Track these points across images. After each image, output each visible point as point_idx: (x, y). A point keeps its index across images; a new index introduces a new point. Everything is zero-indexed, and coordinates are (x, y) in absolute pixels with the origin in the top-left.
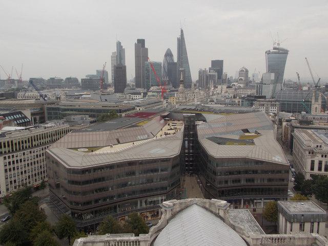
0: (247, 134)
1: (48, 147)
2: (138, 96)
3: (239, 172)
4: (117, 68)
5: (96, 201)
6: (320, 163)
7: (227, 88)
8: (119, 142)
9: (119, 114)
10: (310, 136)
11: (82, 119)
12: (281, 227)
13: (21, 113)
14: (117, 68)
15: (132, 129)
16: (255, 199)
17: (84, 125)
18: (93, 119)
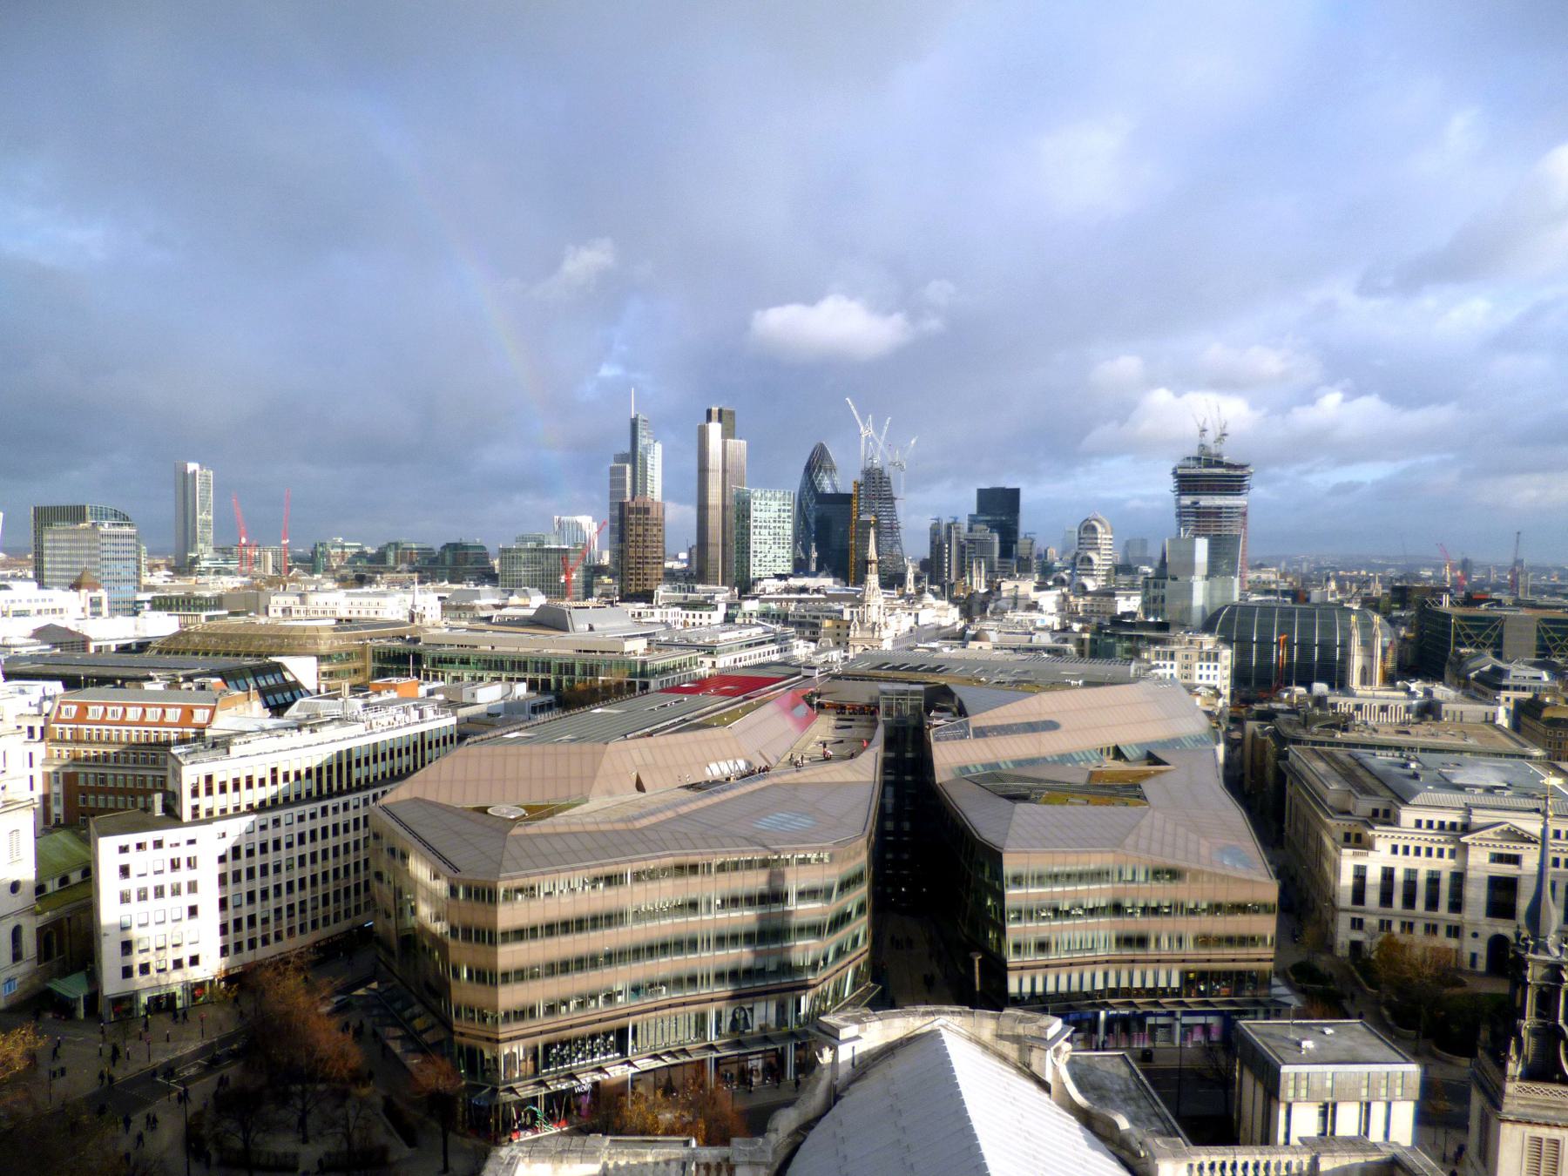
1: (375, 797)
2: (705, 614)
12: (1247, 1123)
13: (279, 668)
16: (1151, 1014)
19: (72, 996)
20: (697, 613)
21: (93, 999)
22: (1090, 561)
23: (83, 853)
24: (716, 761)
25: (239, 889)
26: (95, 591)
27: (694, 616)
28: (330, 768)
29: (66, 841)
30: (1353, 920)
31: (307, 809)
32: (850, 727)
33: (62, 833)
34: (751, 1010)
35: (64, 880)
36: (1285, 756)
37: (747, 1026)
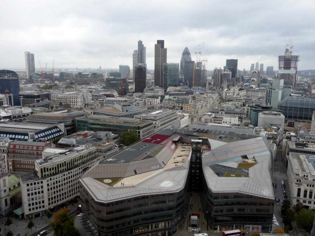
0: (246, 160)
2: (155, 99)
3: (233, 204)
4: (138, 69)
5: (117, 226)
6: (306, 192)
7: (239, 90)
8: (136, 173)
9: (137, 131)
10: (301, 164)
11: (107, 135)
13: (56, 127)
14: (138, 69)
15: (147, 160)
17: (108, 145)
18: (116, 135)
19: (19, 214)
20: (154, 99)
21: (23, 215)
22: (252, 87)
23: (17, 180)
24: (153, 166)
25: (52, 191)
26: (10, 94)
27: (153, 100)
28: (70, 162)
29: (14, 177)
30: (297, 200)
31: (65, 173)
32: (184, 151)
33: (13, 175)
34: (159, 224)
35: (14, 186)
36: (288, 154)
37: (158, 227)
